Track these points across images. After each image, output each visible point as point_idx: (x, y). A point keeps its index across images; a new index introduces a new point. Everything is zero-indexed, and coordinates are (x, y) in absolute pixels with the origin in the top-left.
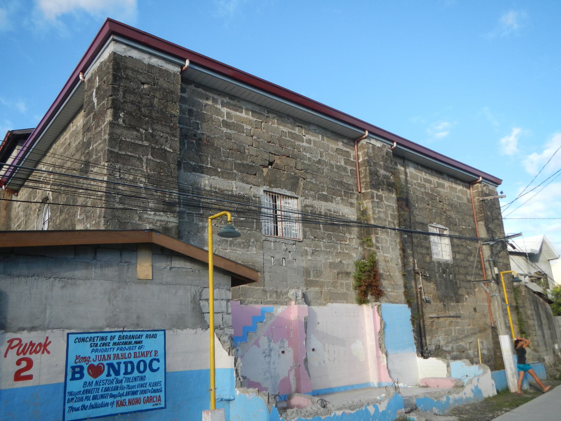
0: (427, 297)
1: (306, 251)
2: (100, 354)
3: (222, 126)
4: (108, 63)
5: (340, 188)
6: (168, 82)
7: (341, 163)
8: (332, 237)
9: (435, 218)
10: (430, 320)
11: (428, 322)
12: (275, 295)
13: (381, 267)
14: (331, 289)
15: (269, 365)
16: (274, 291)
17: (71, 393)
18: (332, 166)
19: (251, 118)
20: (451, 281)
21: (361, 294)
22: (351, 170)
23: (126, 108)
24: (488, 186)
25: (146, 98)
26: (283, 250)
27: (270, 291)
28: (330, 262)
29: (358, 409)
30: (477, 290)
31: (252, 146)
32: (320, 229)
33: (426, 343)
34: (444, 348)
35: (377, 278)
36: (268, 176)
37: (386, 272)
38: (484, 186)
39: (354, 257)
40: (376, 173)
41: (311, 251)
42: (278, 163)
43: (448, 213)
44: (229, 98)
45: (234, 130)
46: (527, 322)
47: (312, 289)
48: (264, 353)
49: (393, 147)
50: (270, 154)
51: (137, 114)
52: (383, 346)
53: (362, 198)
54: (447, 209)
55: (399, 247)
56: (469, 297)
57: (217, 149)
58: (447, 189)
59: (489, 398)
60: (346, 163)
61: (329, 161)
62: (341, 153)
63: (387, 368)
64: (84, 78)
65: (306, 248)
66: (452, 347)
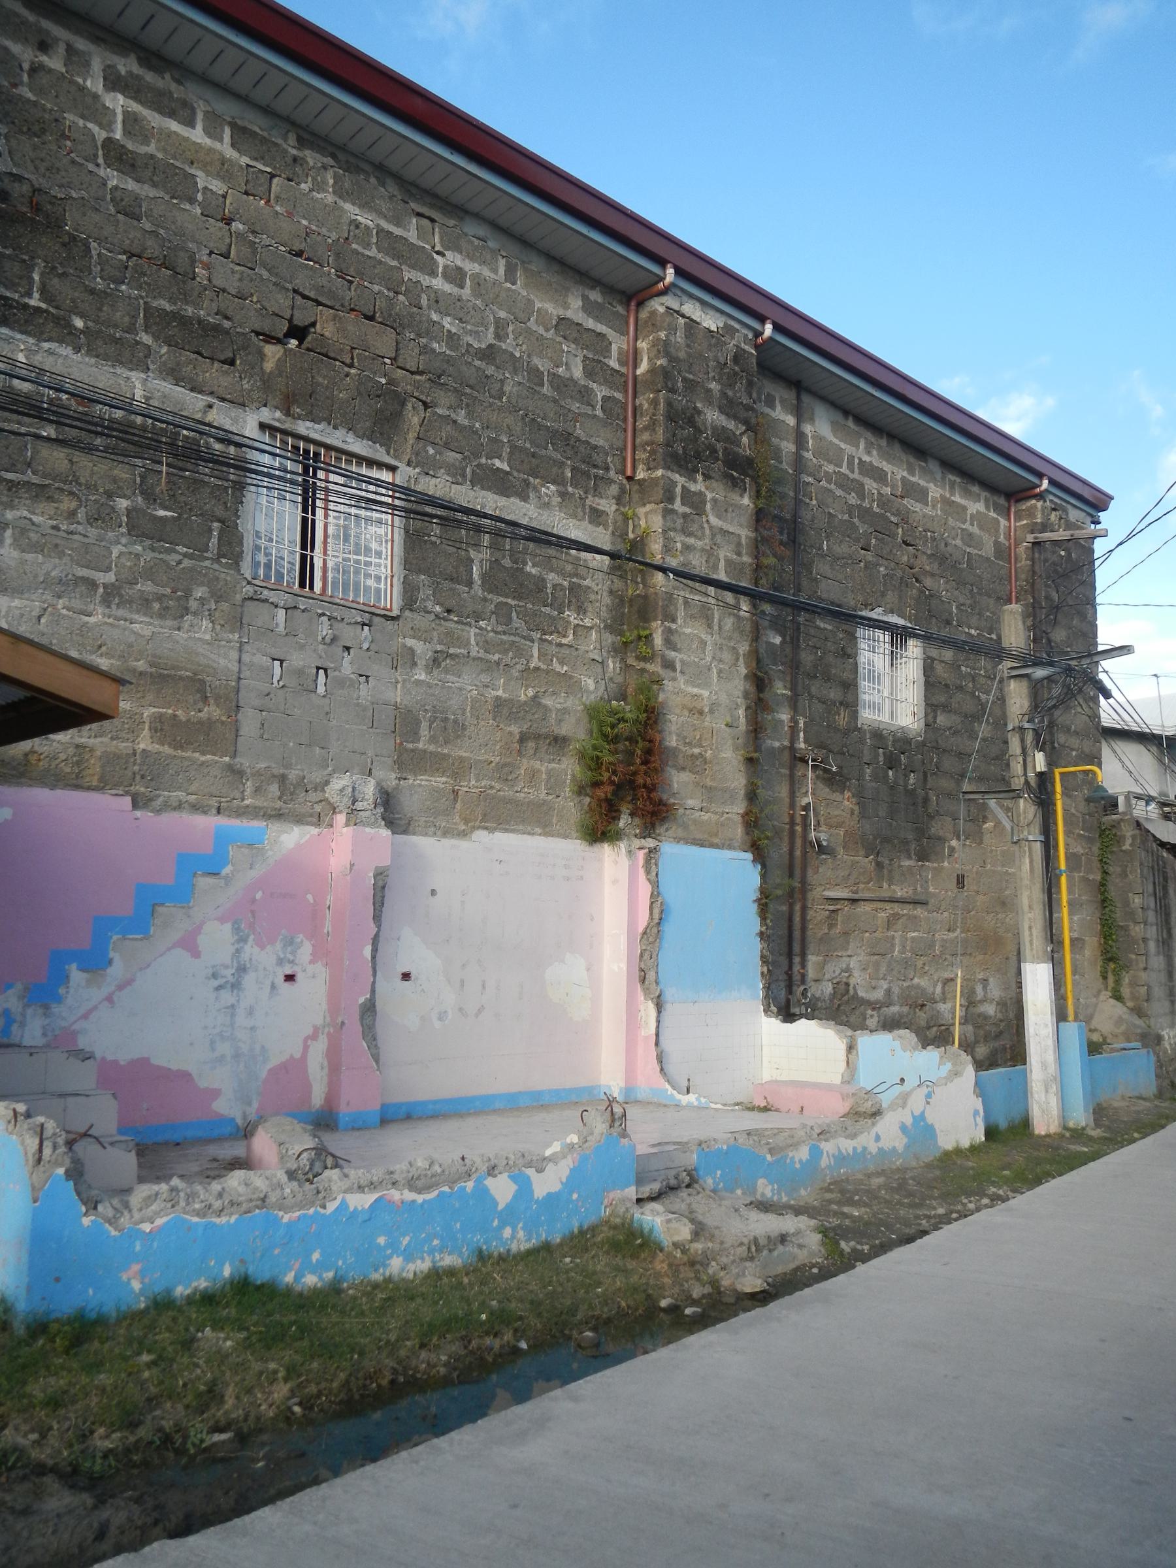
0: (823, 836)
1: (412, 651)
3: (101, 160)
7: (574, 370)
8: (514, 615)
9: (883, 594)
10: (827, 907)
11: (818, 913)
12: (274, 789)
13: (673, 728)
14: (492, 787)
15: (233, 1015)
16: (274, 776)
19: (230, 153)
20: (911, 793)
22: (606, 399)
24: (1065, 511)
26: (320, 638)
27: (258, 774)
28: (498, 698)
29: (446, 1189)
31: (226, 256)
32: (470, 583)
33: (803, 976)
34: (861, 993)
36: (280, 375)
37: (690, 744)
38: (1054, 509)
39: (587, 691)
40: (692, 416)
41: (430, 654)
42: (327, 334)
43: (928, 582)
45: (155, 185)
46: (1125, 929)
47: (423, 780)
48: (215, 976)
50: (298, 298)
52: (651, 976)
53: (636, 497)
54: (928, 568)
55: (743, 671)
57: (76, 248)
58: (934, 506)
59: (958, 1151)
60: (589, 373)
61: (529, 356)
62: (575, 335)
63: (657, 1044)
65: (410, 642)
66: (888, 992)
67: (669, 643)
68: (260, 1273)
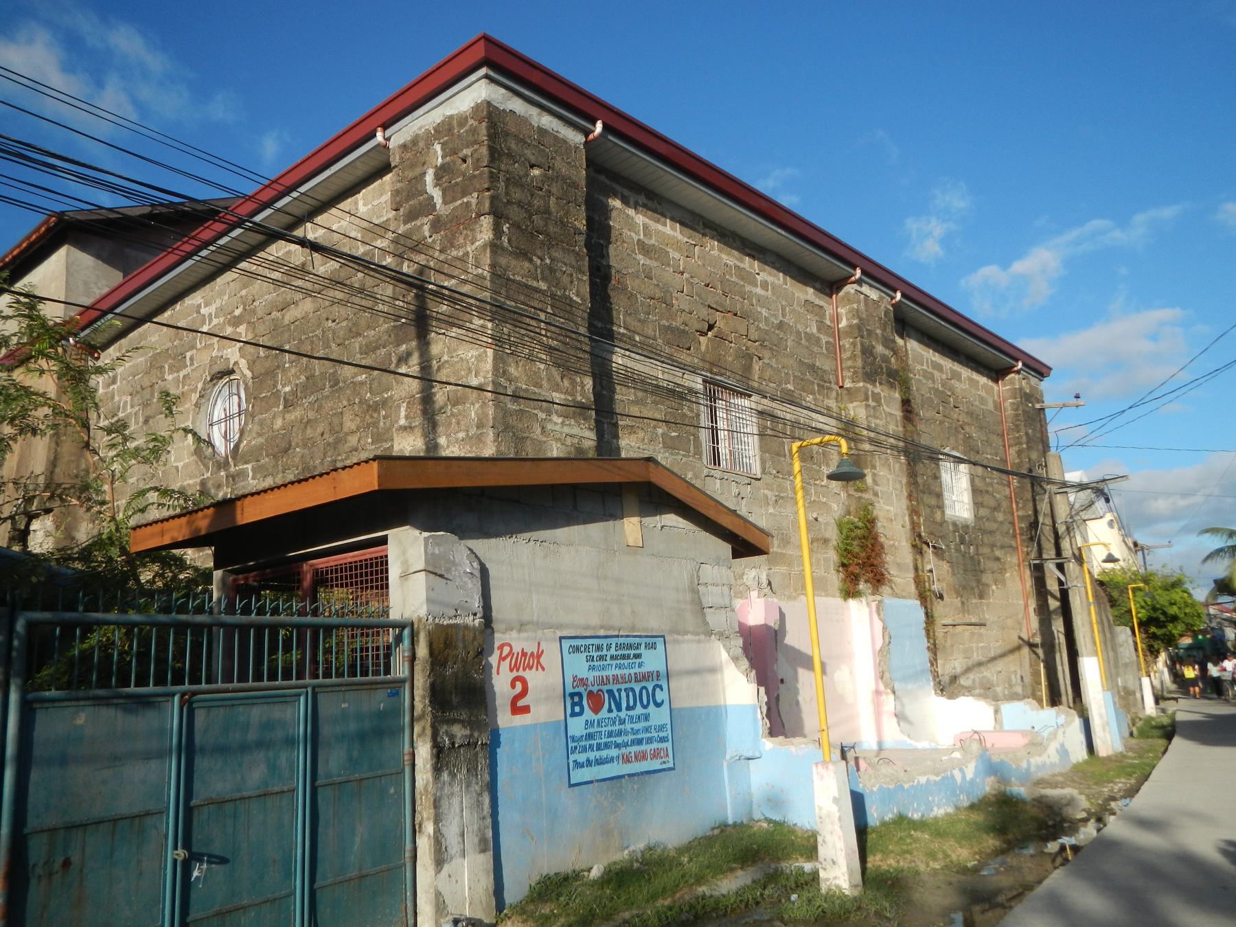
2: (597, 673)
4: (471, 122)
5: (811, 379)
6: (569, 163)
9: (948, 439)
17: (573, 738)
18: (798, 333)
20: (972, 558)
21: (849, 579)
22: (827, 343)
23: (511, 216)
30: (1008, 575)
32: (785, 456)
35: (877, 548)
41: (774, 498)
49: (894, 301)
51: (527, 226)
52: (887, 675)
53: (846, 398)
55: (906, 494)
57: (631, 296)
60: (819, 330)
64: (388, 139)
66: (974, 680)
67: (875, 481)
68: (904, 812)
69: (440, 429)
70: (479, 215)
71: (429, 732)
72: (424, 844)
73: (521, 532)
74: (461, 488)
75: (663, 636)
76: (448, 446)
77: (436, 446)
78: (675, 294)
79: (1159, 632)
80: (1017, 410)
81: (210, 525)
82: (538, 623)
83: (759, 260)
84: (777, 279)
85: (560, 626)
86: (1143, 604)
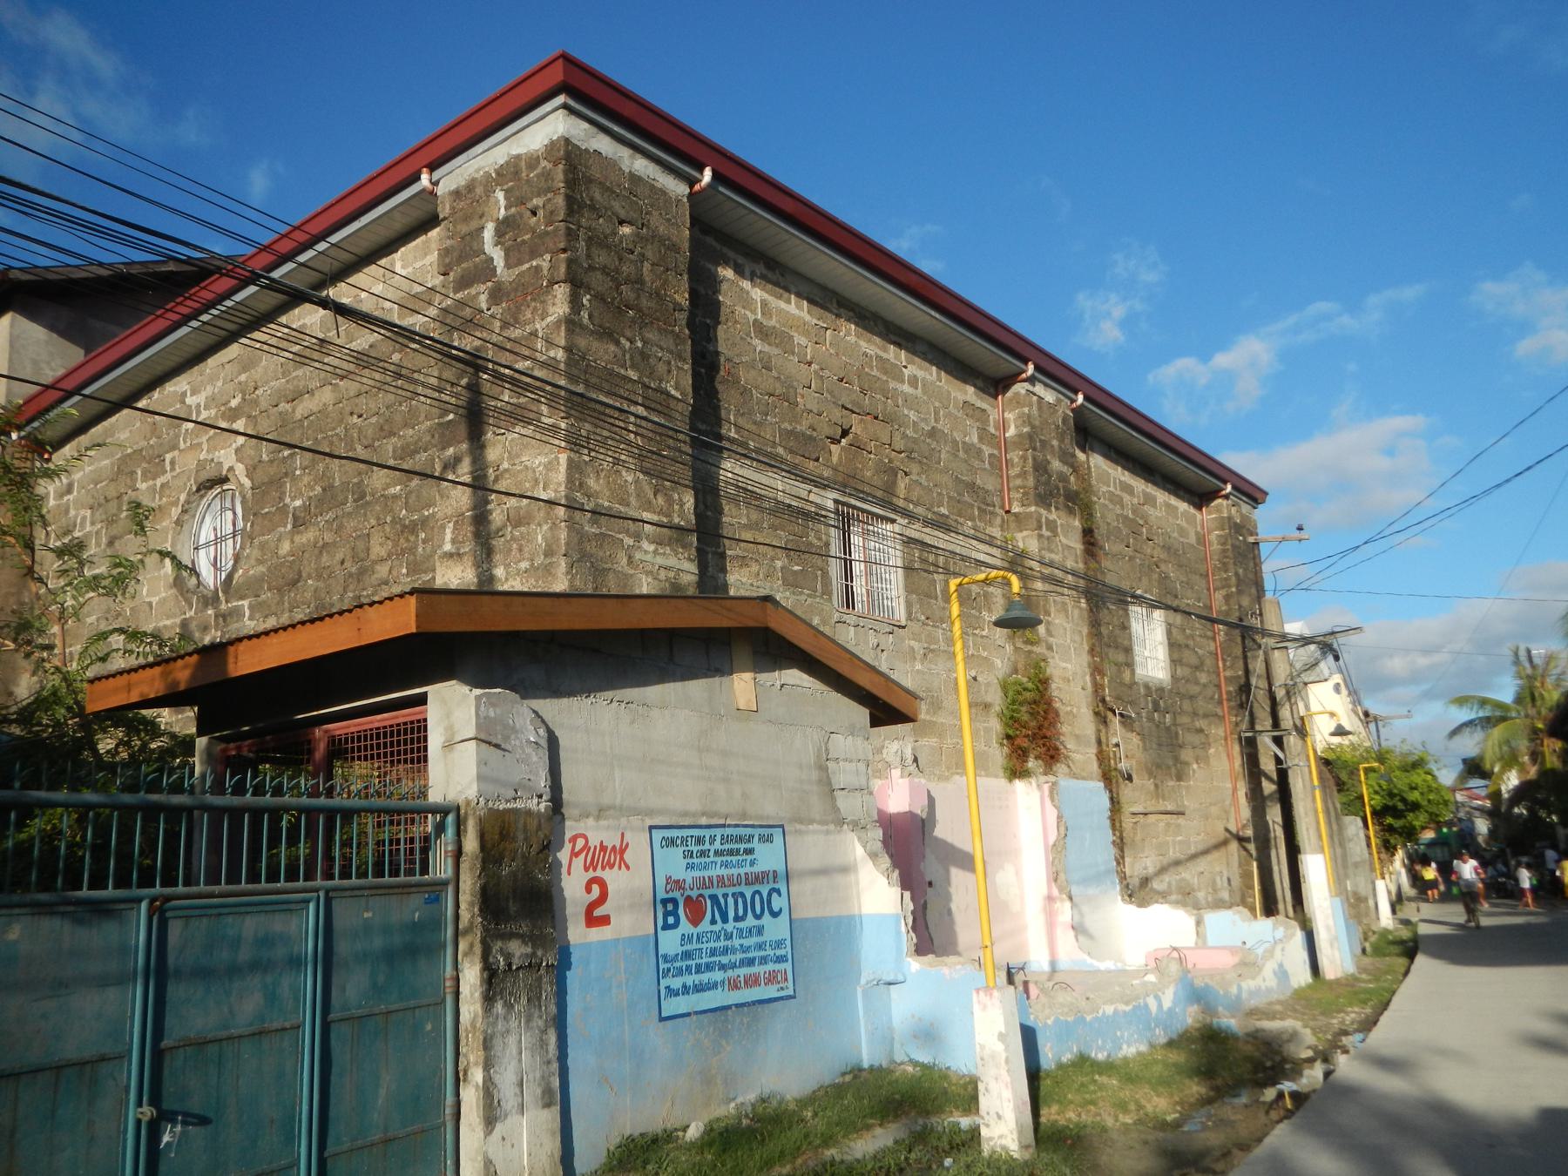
1: (913, 649)
2: (697, 874)
3: (753, 335)
4: (544, 163)
6: (669, 220)
9: (1140, 579)
17: (665, 957)
18: (955, 442)
20: (1168, 729)
22: (991, 455)
23: (593, 284)
24: (1239, 506)
25: (629, 259)
30: (1212, 751)
32: (936, 599)
35: (1051, 716)
44: (764, 263)
51: (614, 299)
52: (1062, 877)
53: (1013, 525)
54: (1161, 556)
56: (1199, 767)
57: (745, 392)
60: (981, 439)
64: (436, 184)
66: (1169, 884)
67: (1049, 632)
69: (497, 557)
70: (552, 283)
71: (478, 949)
72: (470, 1097)
73: (601, 690)
74: (524, 631)
75: (782, 826)
76: (507, 579)
77: (491, 579)
78: (800, 390)
79: (1397, 824)
80: (1224, 544)
81: (193, 677)
82: (621, 808)
83: (907, 349)
84: (930, 374)
85: (650, 812)
86: (1377, 788)
